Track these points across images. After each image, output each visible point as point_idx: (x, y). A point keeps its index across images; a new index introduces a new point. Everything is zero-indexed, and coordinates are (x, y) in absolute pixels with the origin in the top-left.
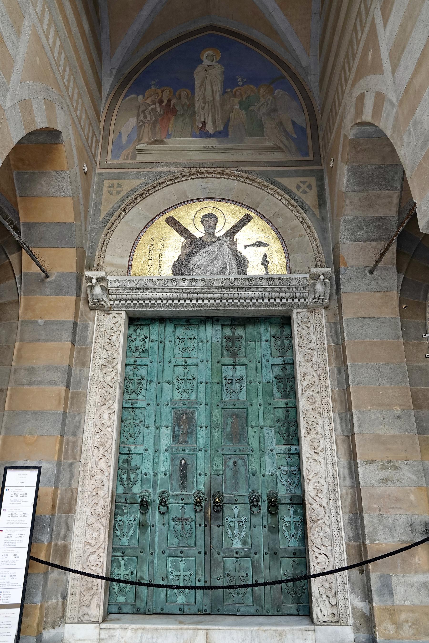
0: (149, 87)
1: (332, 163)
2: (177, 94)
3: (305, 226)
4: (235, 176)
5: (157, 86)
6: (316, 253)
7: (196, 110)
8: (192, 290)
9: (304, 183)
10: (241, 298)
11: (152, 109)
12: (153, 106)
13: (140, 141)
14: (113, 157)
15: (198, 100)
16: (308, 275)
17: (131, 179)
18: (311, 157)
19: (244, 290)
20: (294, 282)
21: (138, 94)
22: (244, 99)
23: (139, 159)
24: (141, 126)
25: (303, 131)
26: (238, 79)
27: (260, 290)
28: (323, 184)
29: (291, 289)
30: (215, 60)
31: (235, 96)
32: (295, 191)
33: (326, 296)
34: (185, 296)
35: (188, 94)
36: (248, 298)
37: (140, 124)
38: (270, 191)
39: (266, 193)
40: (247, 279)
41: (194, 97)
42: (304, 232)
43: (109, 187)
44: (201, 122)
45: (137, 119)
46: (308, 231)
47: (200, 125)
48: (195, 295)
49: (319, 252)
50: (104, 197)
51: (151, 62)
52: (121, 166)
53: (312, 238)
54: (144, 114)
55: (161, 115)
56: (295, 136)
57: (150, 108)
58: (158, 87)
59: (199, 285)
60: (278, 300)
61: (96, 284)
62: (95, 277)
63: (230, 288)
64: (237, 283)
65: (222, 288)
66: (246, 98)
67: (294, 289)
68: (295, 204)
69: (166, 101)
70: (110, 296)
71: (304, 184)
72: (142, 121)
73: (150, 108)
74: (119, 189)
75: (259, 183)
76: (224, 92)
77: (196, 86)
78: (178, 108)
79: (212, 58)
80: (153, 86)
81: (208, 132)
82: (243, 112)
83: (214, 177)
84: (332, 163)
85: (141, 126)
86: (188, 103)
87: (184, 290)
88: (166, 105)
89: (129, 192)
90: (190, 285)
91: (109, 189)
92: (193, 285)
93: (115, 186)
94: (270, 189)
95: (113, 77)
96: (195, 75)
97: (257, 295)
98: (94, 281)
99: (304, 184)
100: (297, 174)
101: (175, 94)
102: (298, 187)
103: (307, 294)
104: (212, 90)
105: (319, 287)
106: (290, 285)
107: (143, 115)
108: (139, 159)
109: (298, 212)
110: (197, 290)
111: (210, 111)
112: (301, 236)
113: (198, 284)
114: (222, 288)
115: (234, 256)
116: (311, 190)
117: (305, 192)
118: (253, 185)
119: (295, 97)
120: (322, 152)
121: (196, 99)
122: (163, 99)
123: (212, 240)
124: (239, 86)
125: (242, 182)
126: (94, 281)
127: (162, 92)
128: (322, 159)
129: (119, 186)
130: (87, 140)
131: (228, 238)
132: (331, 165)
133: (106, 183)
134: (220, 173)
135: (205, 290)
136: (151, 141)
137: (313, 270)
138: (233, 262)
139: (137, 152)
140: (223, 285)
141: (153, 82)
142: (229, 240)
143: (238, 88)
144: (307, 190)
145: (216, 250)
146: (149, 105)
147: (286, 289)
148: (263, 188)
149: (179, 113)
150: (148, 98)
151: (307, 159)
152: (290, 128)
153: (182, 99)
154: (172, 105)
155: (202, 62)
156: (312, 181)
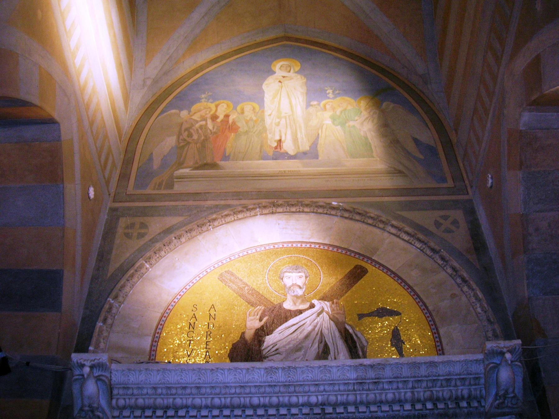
0: (198, 100)
1: (490, 181)
2: (239, 108)
3: (459, 280)
4: (334, 208)
5: (209, 100)
6: (486, 323)
7: (267, 126)
8: (268, 390)
9: (446, 218)
10: (361, 403)
11: (201, 127)
12: (204, 123)
13: (180, 165)
14: (136, 187)
15: (270, 115)
16: (480, 356)
17: (163, 216)
18: (450, 183)
19: (366, 387)
20: (457, 369)
21: (181, 109)
22: (338, 113)
23: (178, 188)
24: (183, 147)
25: (432, 150)
26: (326, 90)
27: (395, 386)
28: (477, 219)
29: (453, 383)
30: (292, 71)
31: (325, 109)
32: (433, 229)
33: (516, 391)
34: (255, 401)
35: (254, 109)
36: (375, 403)
37: (181, 144)
38: (393, 231)
39: (386, 234)
40: (372, 366)
41: (263, 112)
42: (457, 291)
43: (127, 227)
44: (275, 141)
45: (178, 138)
46: (465, 289)
47: (275, 144)
48: (275, 400)
49: (489, 320)
50: (117, 241)
51: (201, 74)
52: (149, 198)
53: (473, 299)
54: (189, 132)
55: (215, 133)
56: (421, 157)
57: (197, 125)
58: (210, 100)
59: (282, 379)
60: (429, 406)
61: (89, 376)
62: (88, 364)
63: (339, 384)
64: (353, 375)
65: (324, 385)
66: (341, 112)
67: (459, 383)
68: (437, 248)
69: (221, 117)
70: (114, 401)
71: (446, 220)
72: (185, 140)
73: (197, 125)
74: (143, 231)
75: (372, 218)
76: (308, 105)
77: (265, 99)
78: (239, 124)
79: (289, 69)
80: (203, 100)
81: (287, 153)
82: (339, 127)
83: (299, 212)
84: (490, 181)
85: (183, 147)
86: (254, 118)
87: (253, 390)
88: (222, 121)
89: (159, 234)
90: (264, 379)
91: (126, 231)
92: (270, 380)
93: (137, 226)
94: (393, 226)
95: (146, 88)
96: (264, 87)
97: (390, 396)
98: (87, 370)
99: (446, 220)
100: (432, 206)
101: (235, 108)
102: (438, 224)
103: (484, 392)
104: (290, 103)
105: (505, 374)
106: (449, 374)
107: (186, 133)
108: (178, 188)
109: (443, 259)
110: (277, 389)
111: (289, 127)
112: (453, 296)
113: (281, 377)
114: (324, 385)
115: (340, 332)
116: (458, 227)
117: (449, 231)
118: (363, 222)
119: (412, 110)
120: (465, 176)
121: (267, 113)
122: (218, 114)
123: (302, 307)
124: (329, 98)
125: (346, 218)
126: (87, 370)
127: (217, 106)
128: (468, 185)
129: (143, 225)
130: (100, 157)
131: (328, 304)
132: (489, 185)
133: (123, 222)
134: (307, 205)
135: (292, 389)
136: (197, 165)
137: (490, 345)
138: (341, 344)
139: (175, 180)
140: (327, 378)
141: (203, 96)
142: (331, 307)
143: (329, 100)
144: (453, 228)
145: (308, 323)
146: (197, 122)
147: (444, 383)
148: (381, 226)
149: (241, 130)
150: (195, 113)
151: (445, 185)
152: (411, 146)
153: (246, 113)
154: (230, 121)
155: (274, 73)
156: (458, 215)
